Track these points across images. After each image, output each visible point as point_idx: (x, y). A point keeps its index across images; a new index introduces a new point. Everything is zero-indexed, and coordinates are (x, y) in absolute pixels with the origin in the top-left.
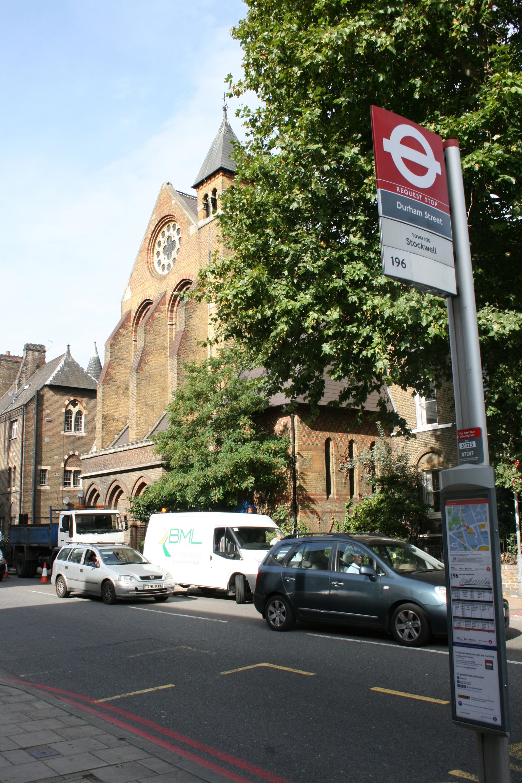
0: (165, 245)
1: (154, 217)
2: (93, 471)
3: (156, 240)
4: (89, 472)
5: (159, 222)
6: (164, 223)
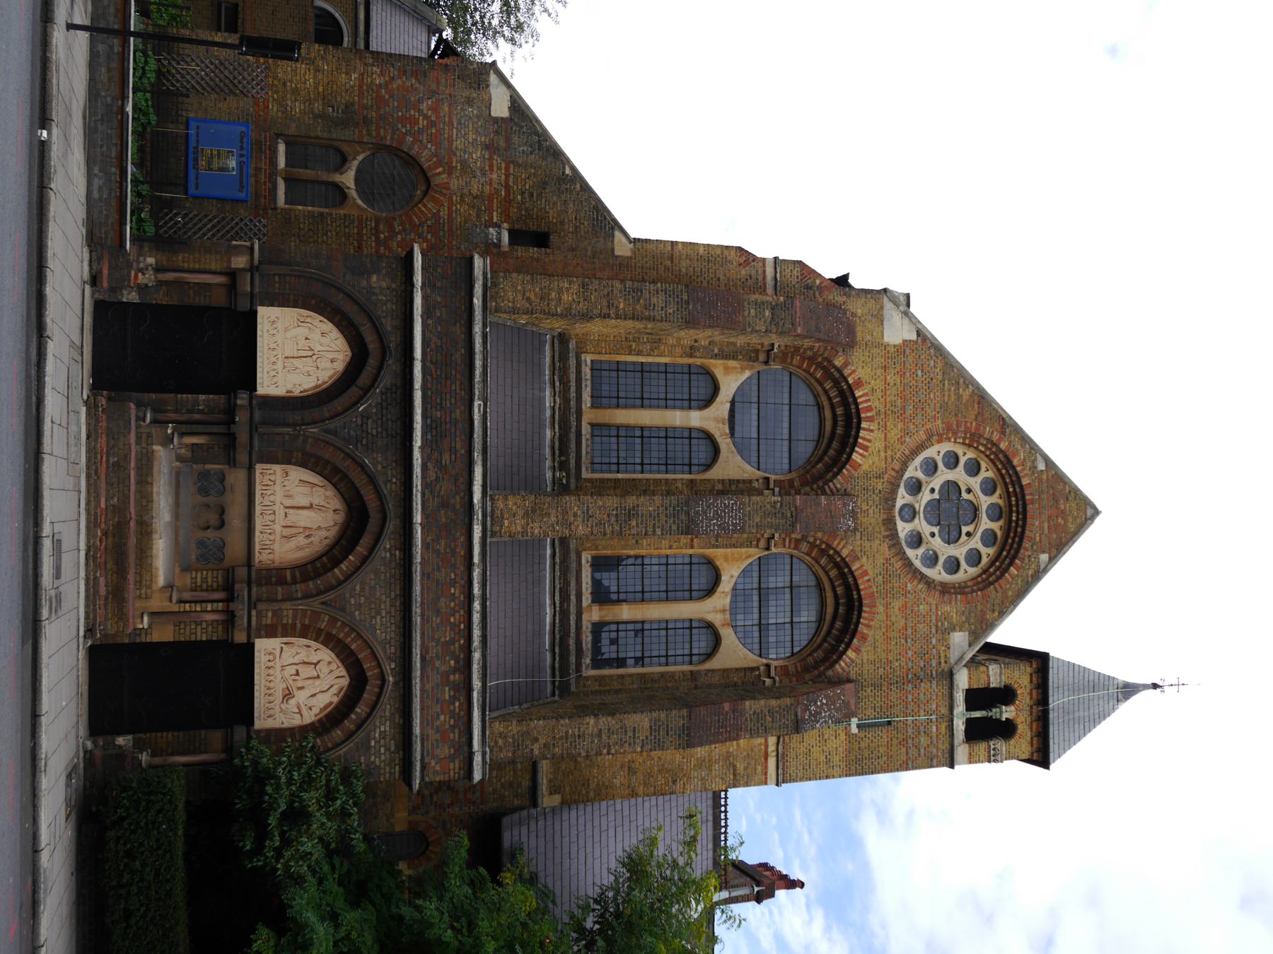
0: (963, 489)
1: (1041, 466)
3: (987, 456)
5: (1021, 487)
6: (1013, 499)
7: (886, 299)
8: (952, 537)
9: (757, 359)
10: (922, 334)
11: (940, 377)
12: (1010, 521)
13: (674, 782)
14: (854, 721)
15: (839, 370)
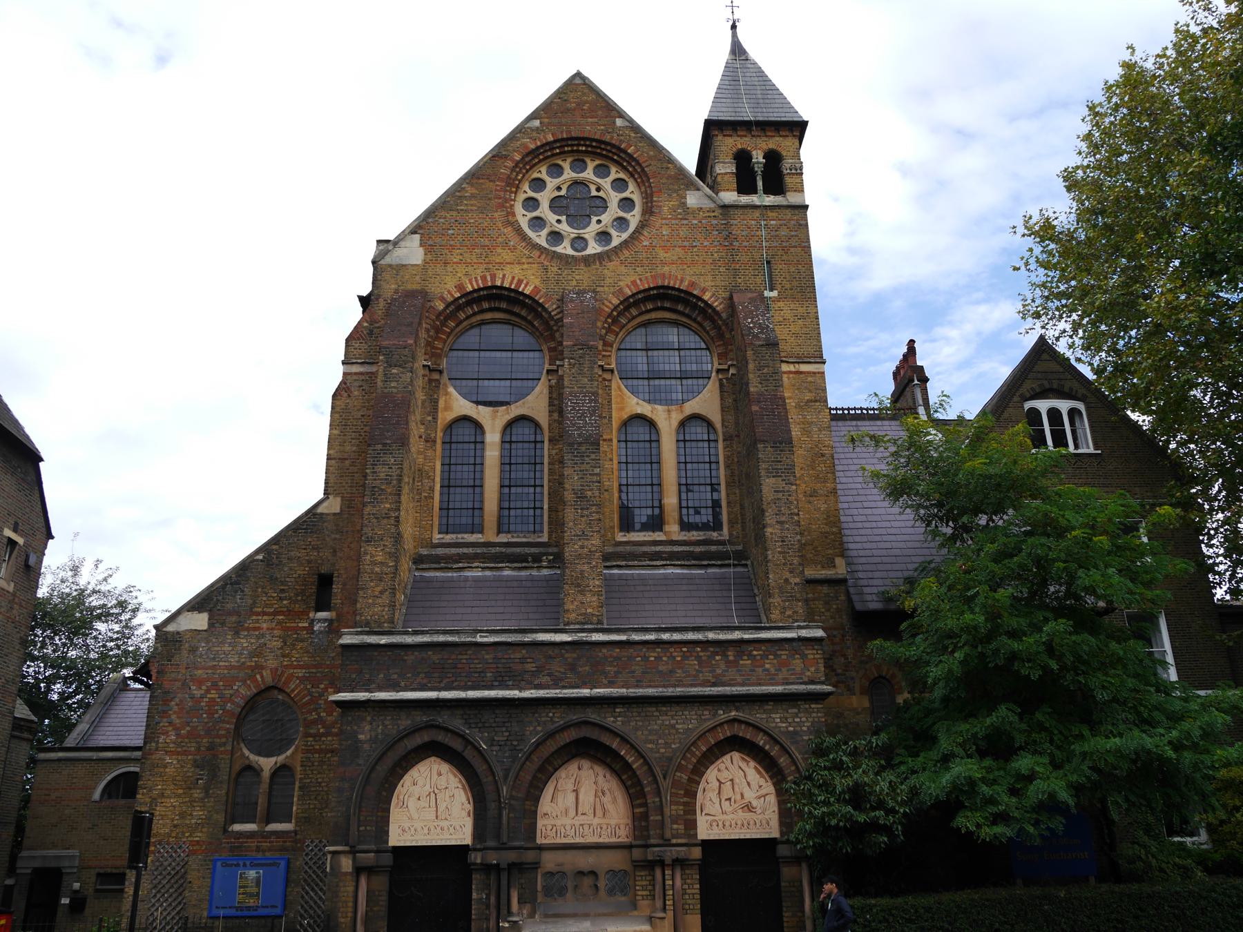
1: (537, 123)
2: (423, 688)
3: (527, 171)
4: (395, 687)
5: (555, 141)
6: (566, 149)
7: (382, 262)
8: (601, 205)
9: (438, 381)
10: (415, 229)
11: (455, 214)
12: (586, 152)
13: (823, 455)
14: (767, 293)
15: (448, 306)
